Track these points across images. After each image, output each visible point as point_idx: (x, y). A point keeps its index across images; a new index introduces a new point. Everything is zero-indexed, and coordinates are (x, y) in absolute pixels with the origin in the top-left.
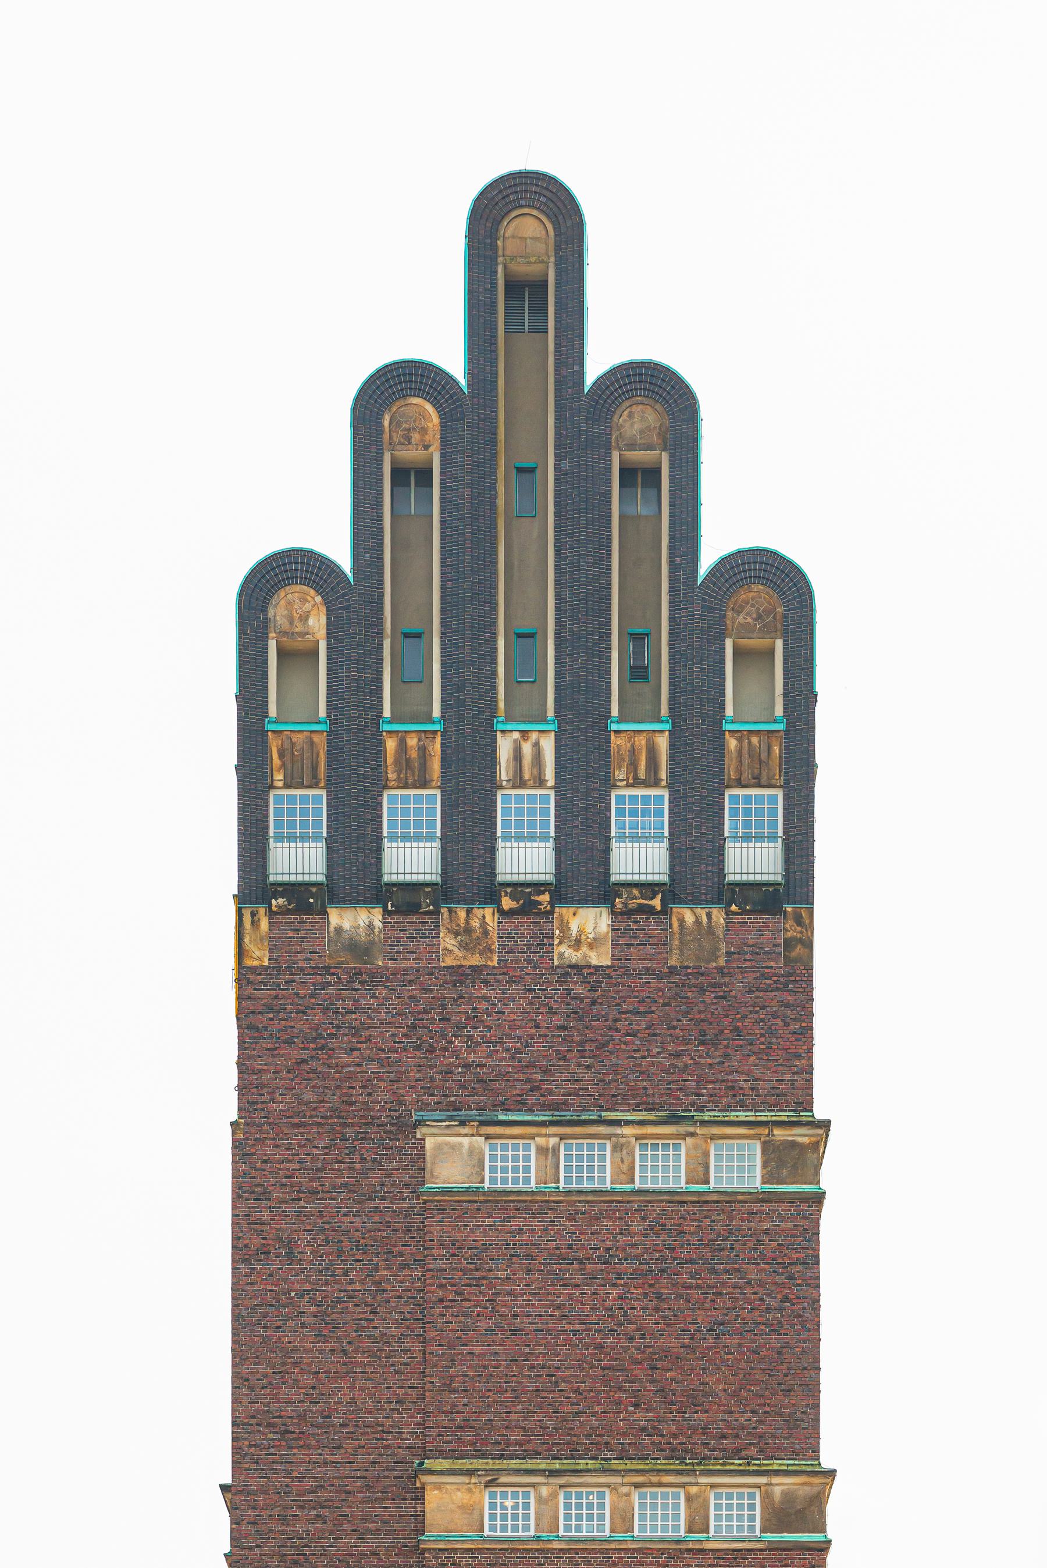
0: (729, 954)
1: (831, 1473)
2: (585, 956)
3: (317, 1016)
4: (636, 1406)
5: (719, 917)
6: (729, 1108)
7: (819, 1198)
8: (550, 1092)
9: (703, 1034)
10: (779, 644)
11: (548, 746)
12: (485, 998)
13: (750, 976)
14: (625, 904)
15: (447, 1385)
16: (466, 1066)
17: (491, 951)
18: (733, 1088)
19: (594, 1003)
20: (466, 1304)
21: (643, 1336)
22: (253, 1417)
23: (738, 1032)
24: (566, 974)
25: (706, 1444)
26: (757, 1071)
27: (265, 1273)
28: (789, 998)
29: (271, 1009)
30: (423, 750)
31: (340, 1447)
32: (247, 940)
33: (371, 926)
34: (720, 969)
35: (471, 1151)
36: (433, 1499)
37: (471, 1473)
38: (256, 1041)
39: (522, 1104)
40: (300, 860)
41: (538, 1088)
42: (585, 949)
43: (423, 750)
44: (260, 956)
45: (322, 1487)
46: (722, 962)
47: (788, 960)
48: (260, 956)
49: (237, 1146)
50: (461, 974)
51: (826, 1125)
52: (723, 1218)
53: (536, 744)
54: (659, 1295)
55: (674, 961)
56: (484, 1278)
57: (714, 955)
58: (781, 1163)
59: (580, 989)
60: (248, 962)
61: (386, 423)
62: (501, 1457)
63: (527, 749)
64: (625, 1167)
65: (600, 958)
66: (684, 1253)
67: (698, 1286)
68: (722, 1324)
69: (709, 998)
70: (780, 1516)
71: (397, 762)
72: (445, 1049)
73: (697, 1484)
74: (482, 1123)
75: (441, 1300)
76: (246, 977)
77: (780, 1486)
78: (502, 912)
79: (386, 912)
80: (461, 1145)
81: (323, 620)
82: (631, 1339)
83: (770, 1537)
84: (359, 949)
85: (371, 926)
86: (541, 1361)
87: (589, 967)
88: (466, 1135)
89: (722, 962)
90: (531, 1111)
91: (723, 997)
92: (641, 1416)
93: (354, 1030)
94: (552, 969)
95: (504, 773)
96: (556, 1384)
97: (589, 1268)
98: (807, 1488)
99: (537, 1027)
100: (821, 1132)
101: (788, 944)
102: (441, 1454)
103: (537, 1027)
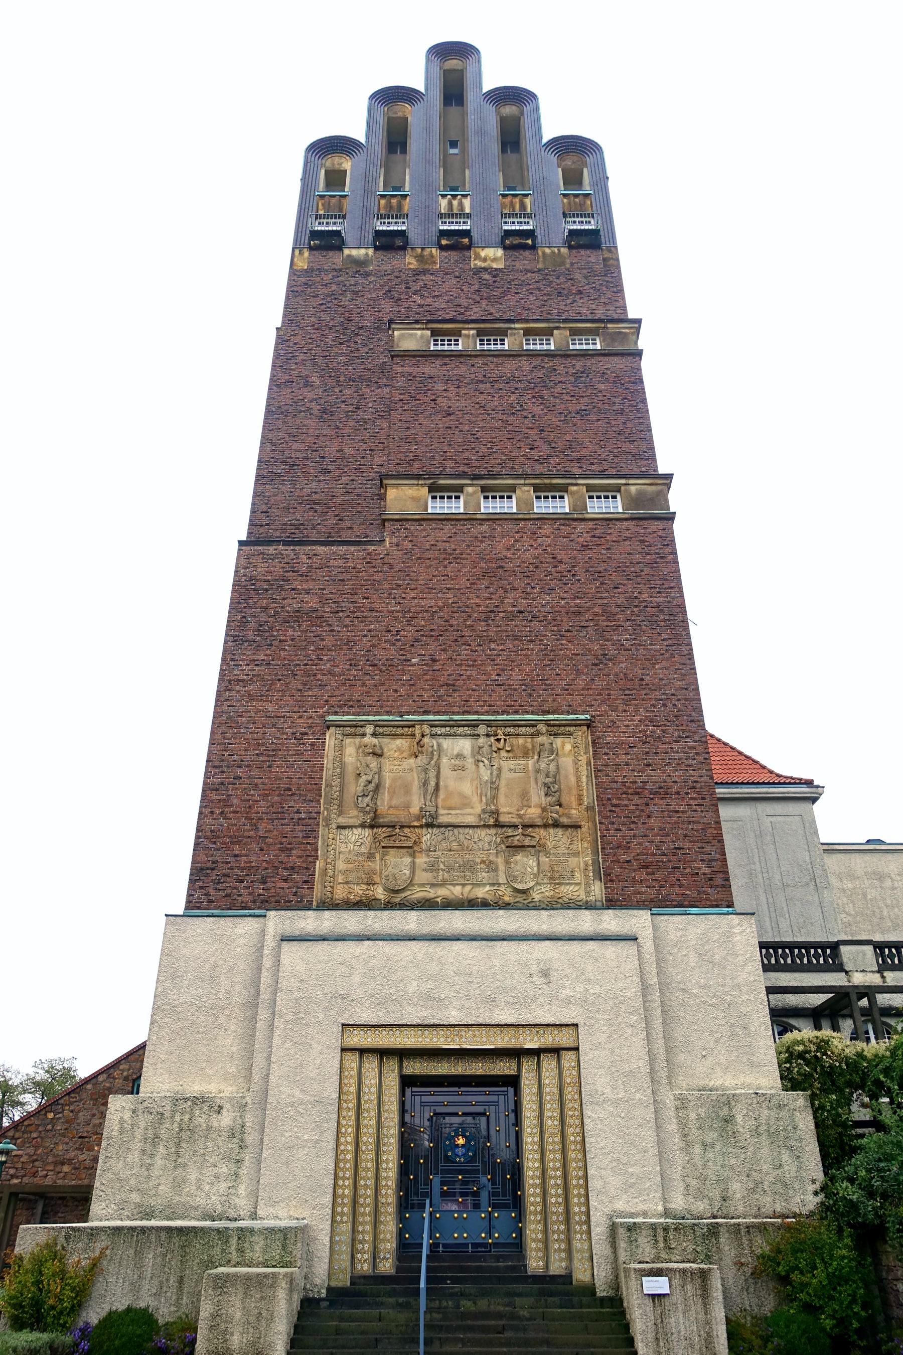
1: (669, 477)
3: (334, 287)
4: (531, 449)
5: (564, 251)
7: (639, 354)
13: (585, 271)
15: (406, 440)
16: (420, 306)
17: (435, 263)
21: (533, 416)
22: (272, 458)
29: (307, 284)
31: (329, 472)
32: (296, 260)
33: (367, 254)
34: (568, 270)
36: (391, 493)
41: (463, 314)
44: (302, 264)
45: (316, 493)
47: (605, 266)
50: (417, 273)
51: (639, 321)
53: (460, 200)
54: (542, 397)
55: (540, 266)
56: (429, 390)
57: (563, 263)
58: (613, 340)
59: (486, 277)
60: (295, 268)
63: (455, 203)
64: (517, 342)
65: (500, 265)
67: (568, 393)
69: (562, 279)
70: (634, 502)
73: (576, 485)
74: (429, 321)
75: (401, 400)
76: (293, 272)
78: (442, 248)
80: (416, 334)
81: (350, 164)
84: (360, 263)
85: (367, 254)
86: (467, 428)
88: (419, 329)
89: (568, 266)
91: (571, 279)
92: (535, 454)
93: (356, 293)
94: (470, 270)
98: (653, 488)
100: (636, 325)
101: (604, 260)
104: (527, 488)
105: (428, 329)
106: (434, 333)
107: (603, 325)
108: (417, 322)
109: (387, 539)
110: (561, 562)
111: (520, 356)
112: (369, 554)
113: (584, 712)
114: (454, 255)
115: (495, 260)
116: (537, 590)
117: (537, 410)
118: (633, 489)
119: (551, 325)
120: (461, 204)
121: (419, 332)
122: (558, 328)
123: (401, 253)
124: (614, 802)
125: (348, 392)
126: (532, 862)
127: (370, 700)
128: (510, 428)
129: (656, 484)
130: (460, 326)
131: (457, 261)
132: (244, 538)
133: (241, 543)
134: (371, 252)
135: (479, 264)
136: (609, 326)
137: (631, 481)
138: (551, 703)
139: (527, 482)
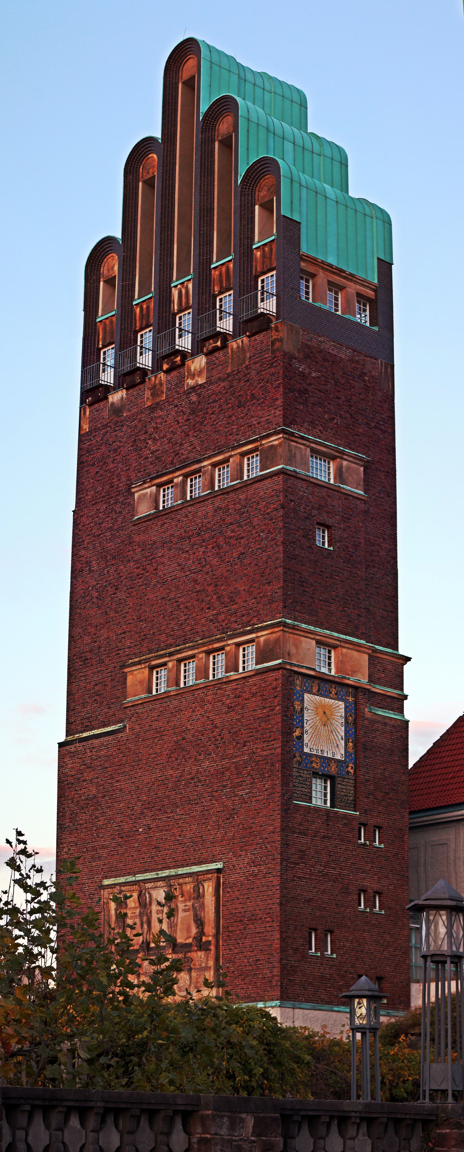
2: (196, 381)
6: (250, 437)
8: (182, 454)
10: (275, 198)
12: (160, 416)
14: (207, 349)
17: (163, 392)
18: (251, 426)
20: (147, 574)
23: (253, 396)
24: (190, 393)
30: (148, 308)
36: (130, 679)
37: (139, 663)
42: (196, 378)
43: (148, 308)
48: (86, 427)
50: (152, 409)
52: (242, 497)
59: (194, 398)
63: (184, 291)
66: (229, 519)
68: (244, 553)
73: (228, 645)
74: (152, 479)
77: (263, 636)
79: (127, 389)
80: (147, 493)
88: (148, 487)
89: (247, 363)
96: (179, 606)
98: (274, 635)
104: (201, 656)
105: (153, 485)
106: (159, 486)
107: (259, 444)
108: (145, 482)
110: (216, 727)
111: (207, 500)
113: (220, 860)
114: (174, 374)
115: (200, 373)
116: (202, 757)
117: (215, 562)
118: (262, 639)
119: (227, 455)
121: (148, 490)
122: (231, 456)
123: (141, 386)
124: (231, 929)
126: (187, 977)
127: (121, 865)
128: (198, 588)
129: (275, 632)
130: (170, 476)
132: (62, 738)
133: (61, 745)
134: (124, 391)
135: (190, 382)
136: (263, 442)
137: (260, 634)
138: (205, 855)
139: (200, 650)
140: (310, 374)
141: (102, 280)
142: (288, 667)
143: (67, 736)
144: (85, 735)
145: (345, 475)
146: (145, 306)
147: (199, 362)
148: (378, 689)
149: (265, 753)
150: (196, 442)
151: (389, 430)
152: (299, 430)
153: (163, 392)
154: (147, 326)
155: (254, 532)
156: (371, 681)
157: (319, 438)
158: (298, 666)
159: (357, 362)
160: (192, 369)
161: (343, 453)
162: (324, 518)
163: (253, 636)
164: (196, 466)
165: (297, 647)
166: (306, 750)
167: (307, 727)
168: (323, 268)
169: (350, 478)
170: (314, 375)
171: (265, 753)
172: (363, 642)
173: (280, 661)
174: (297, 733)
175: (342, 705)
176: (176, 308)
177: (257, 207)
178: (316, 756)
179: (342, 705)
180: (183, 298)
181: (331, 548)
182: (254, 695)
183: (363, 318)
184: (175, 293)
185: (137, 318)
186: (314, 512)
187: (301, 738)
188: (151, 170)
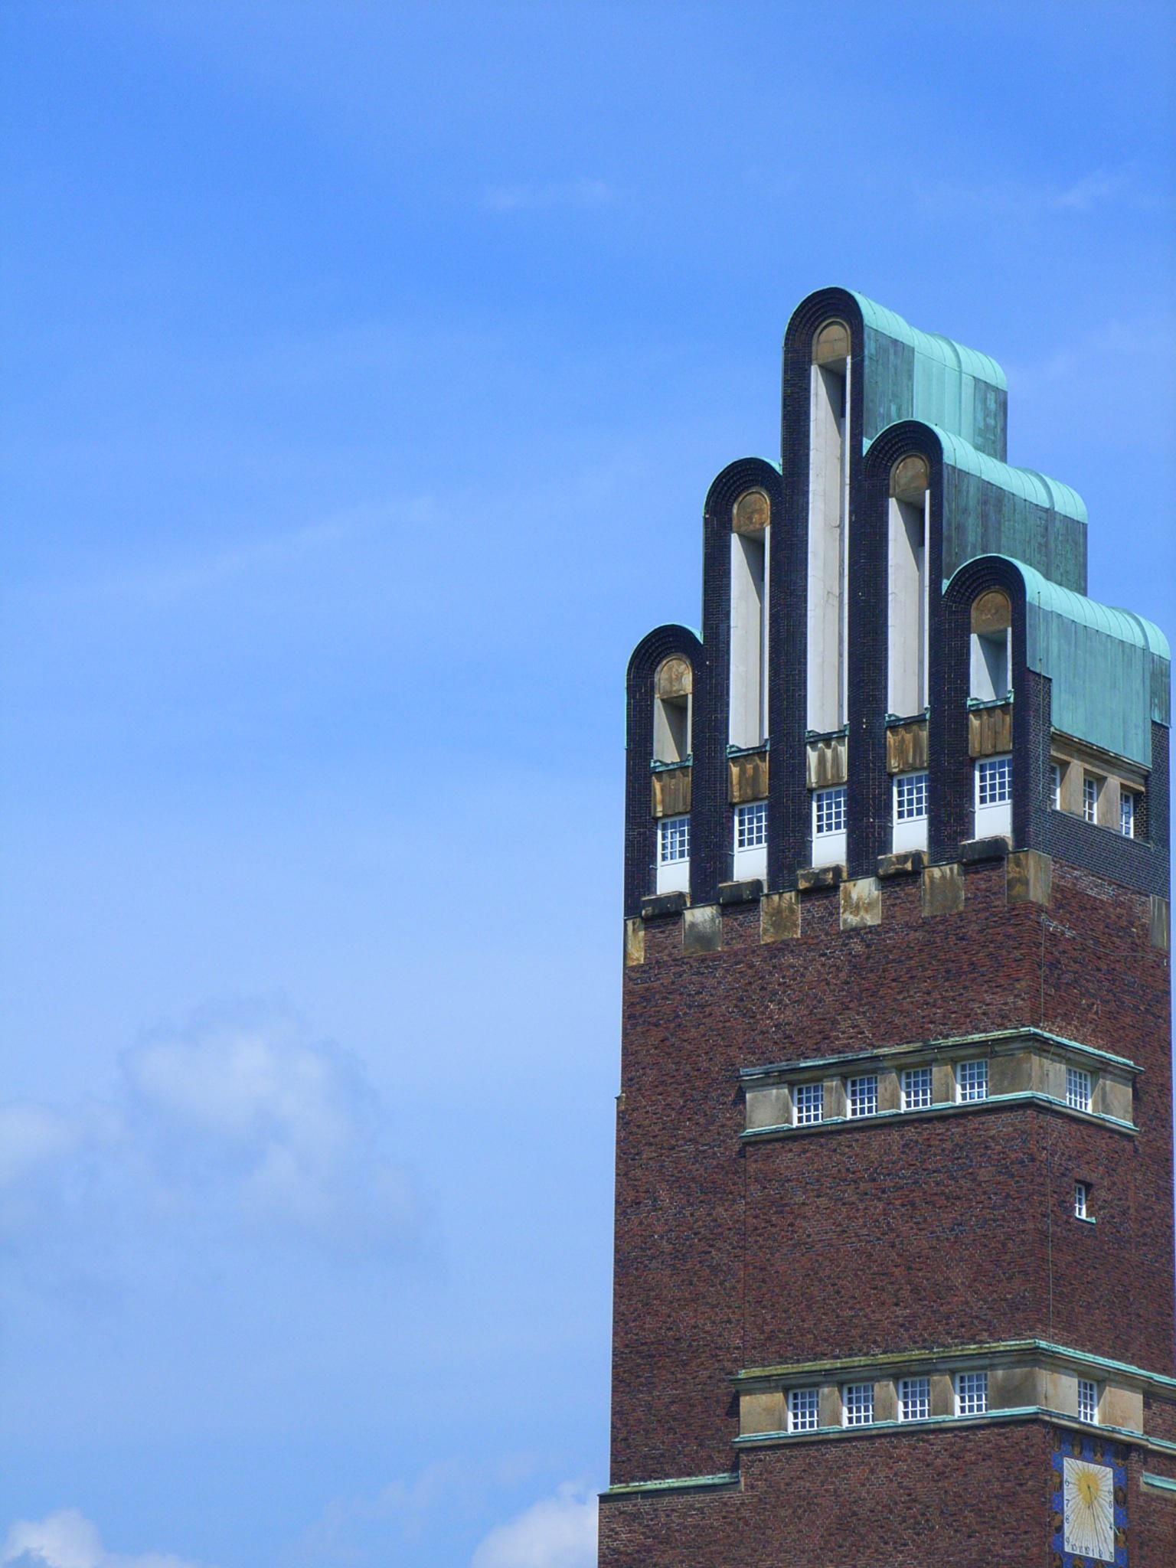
0: (967, 899)
2: (862, 918)
8: (838, 1038)
9: (948, 971)
10: (1010, 630)
11: (843, 750)
17: (796, 926)
19: (868, 958)
20: (774, 1230)
25: (948, 1333)
26: (988, 998)
27: (636, 1222)
28: (1011, 930)
34: (960, 914)
35: (778, 1098)
36: (745, 1401)
38: (634, 1026)
39: (818, 1052)
40: (673, 875)
42: (862, 913)
46: (961, 908)
48: (638, 956)
49: (621, 1116)
50: (776, 950)
53: (835, 750)
54: (912, 1204)
55: (926, 914)
59: (858, 947)
60: (631, 963)
61: (735, 511)
62: (798, 1361)
63: (829, 753)
65: (872, 919)
71: (740, 783)
72: (763, 1013)
82: (893, 1246)
83: (994, 1413)
84: (703, 940)
87: (865, 927)
89: (961, 908)
90: (823, 1056)
94: (839, 934)
95: (813, 778)
97: (862, 1186)
99: (828, 984)
101: (1011, 884)
102: (754, 1363)
103: (828, 984)
109: (742, 1479)
112: (725, 1504)
116: (890, 1547)
120: (836, 757)
125: (701, 1212)
131: (821, 918)
132: (606, 1488)
133: (604, 1499)
135: (850, 919)
140: (1063, 933)
141: (657, 696)
142: (1047, 1418)
143: (612, 1483)
144: (651, 1485)
145: (1110, 1098)
146: (749, 767)
147: (865, 889)
148: (1157, 1444)
149: (1008, 1553)
150: (860, 1020)
151: (1164, 1013)
152: (1051, 1031)
153: (796, 926)
154: (756, 799)
155: (979, 1191)
156: (1146, 1433)
157: (1075, 1039)
158: (1058, 1416)
159: (1121, 905)
160: (854, 896)
161: (1107, 1063)
162: (1083, 1173)
163: (986, 1362)
164: (869, 1065)
165: (1056, 1386)
166: (1068, 1549)
167: (1068, 1510)
168: (1079, 751)
169: (1116, 1103)
170: (1068, 934)
171: (1008, 1553)
172: (1133, 1369)
173: (1031, 1409)
174: (1056, 1523)
175: (1109, 1472)
176: (814, 779)
177: (974, 638)
178: (1080, 1557)
179: (1109, 1472)
180: (829, 765)
181: (1093, 1220)
182: (987, 1457)
183: (1128, 827)
184: (812, 756)
185: (735, 781)
186: (1071, 1165)
187: (1060, 1529)
188: (756, 517)
